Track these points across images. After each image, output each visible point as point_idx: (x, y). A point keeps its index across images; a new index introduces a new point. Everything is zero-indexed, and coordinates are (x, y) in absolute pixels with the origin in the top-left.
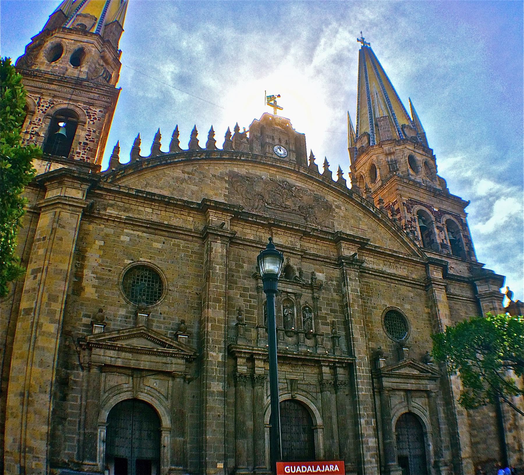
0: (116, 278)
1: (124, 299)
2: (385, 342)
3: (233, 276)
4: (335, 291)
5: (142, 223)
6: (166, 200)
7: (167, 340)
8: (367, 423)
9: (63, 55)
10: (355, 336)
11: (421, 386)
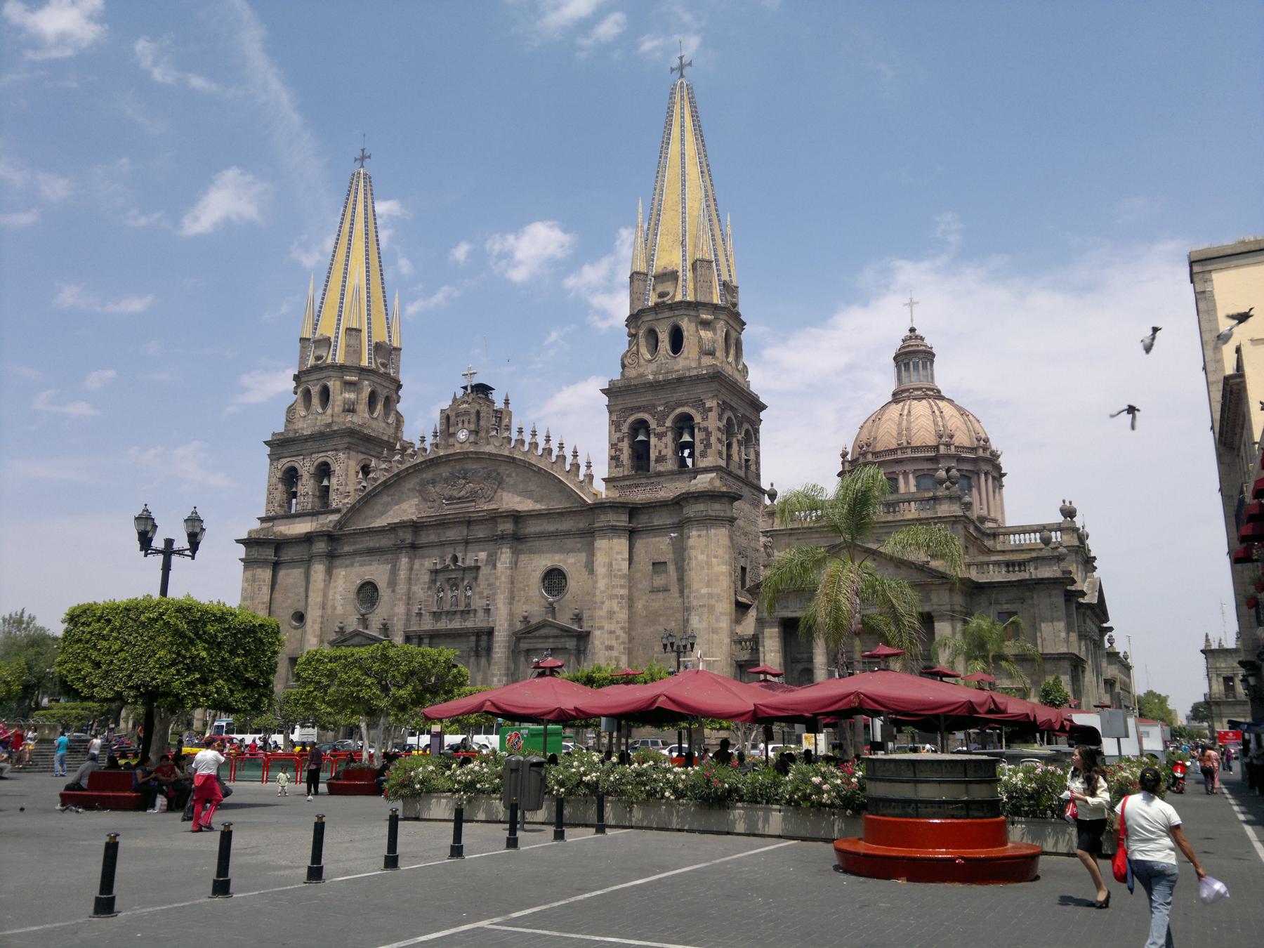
0: (352, 595)
8: (499, 681)
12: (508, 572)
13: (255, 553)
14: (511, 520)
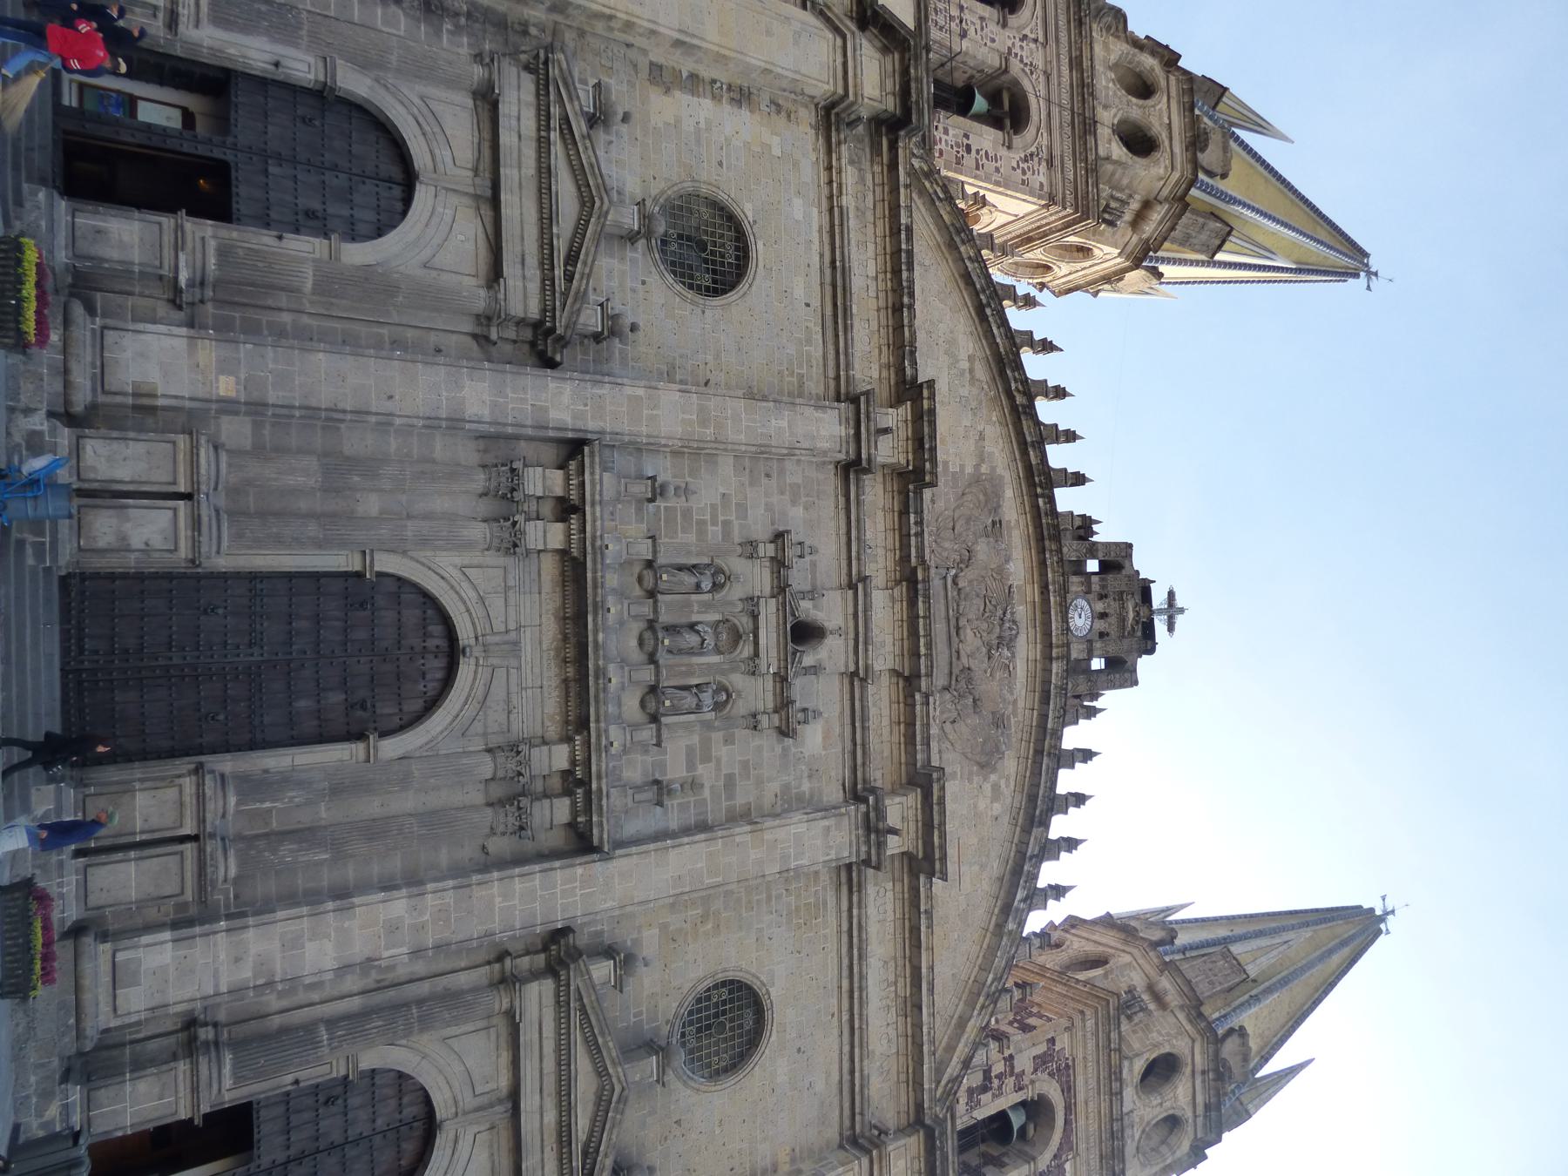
1: (663, 192)
2: (663, 988)
3: (768, 475)
4: (786, 788)
5: (842, 247)
6: (906, 300)
7: (585, 263)
8: (393, 928)
9: (1134, 100)
10: (672, 853)
11: (538, 1156)
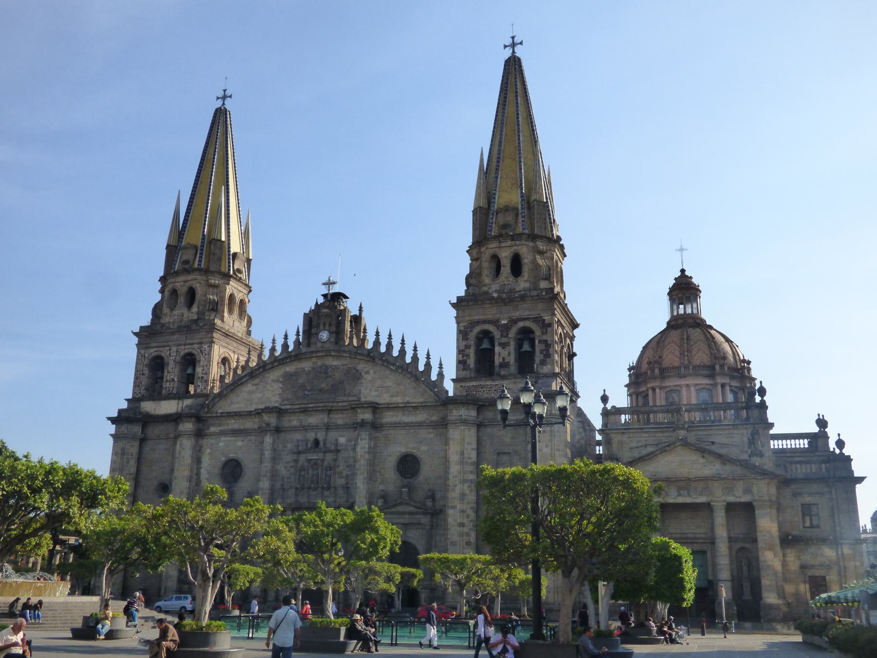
0: (217, 471)
12: (367, 456)
13: (124, 428)
14: (370, 410)
